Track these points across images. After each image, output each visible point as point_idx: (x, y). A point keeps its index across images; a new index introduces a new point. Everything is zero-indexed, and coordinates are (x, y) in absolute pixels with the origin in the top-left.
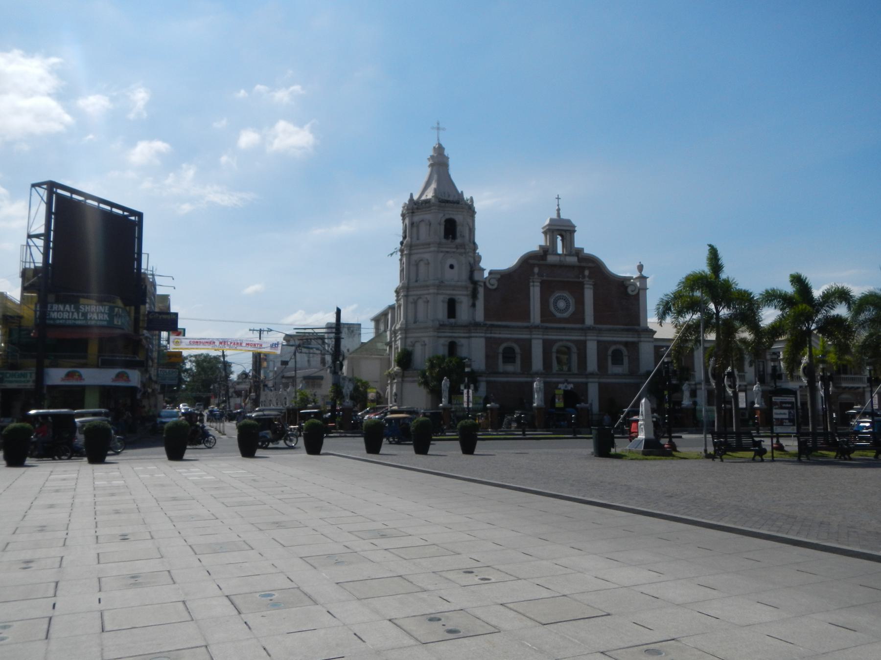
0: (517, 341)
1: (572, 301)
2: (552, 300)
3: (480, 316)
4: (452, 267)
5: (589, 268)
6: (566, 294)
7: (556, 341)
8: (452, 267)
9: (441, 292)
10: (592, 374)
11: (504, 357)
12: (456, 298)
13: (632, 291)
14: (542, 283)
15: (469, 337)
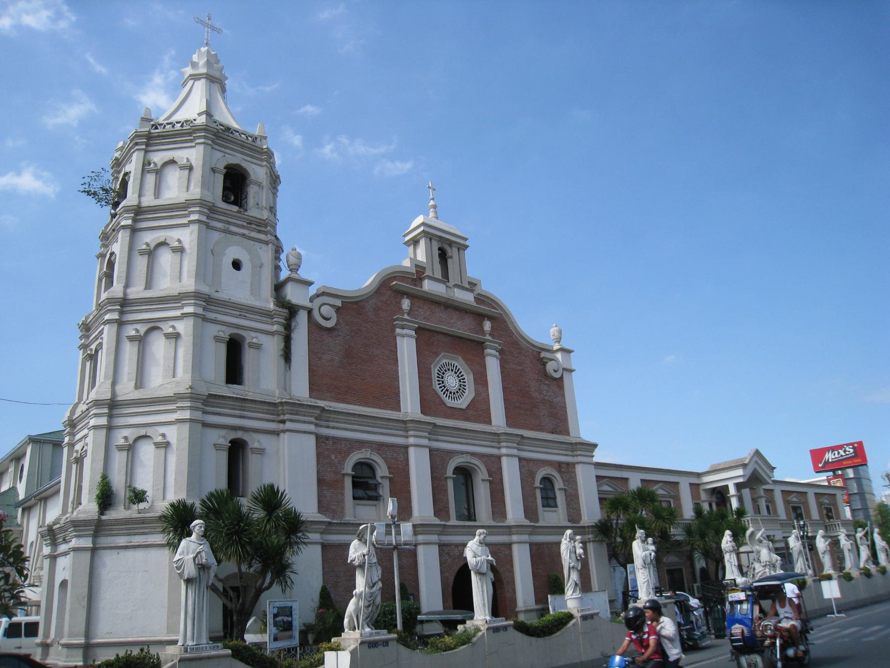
0: (380, 447)
1: (469, 378)
2: (435, 372)
3: (300, 388)
4: (237, 265)
5: (491, 318)
6: (459, 363)
7: (452, 453)
8: (237, 265)
9: (212, 315)
10: (518, 529)
11: (355, 485)
12: (250, 337)
13: (555, 371)
14: (419, 331)
15: (277, 433)
